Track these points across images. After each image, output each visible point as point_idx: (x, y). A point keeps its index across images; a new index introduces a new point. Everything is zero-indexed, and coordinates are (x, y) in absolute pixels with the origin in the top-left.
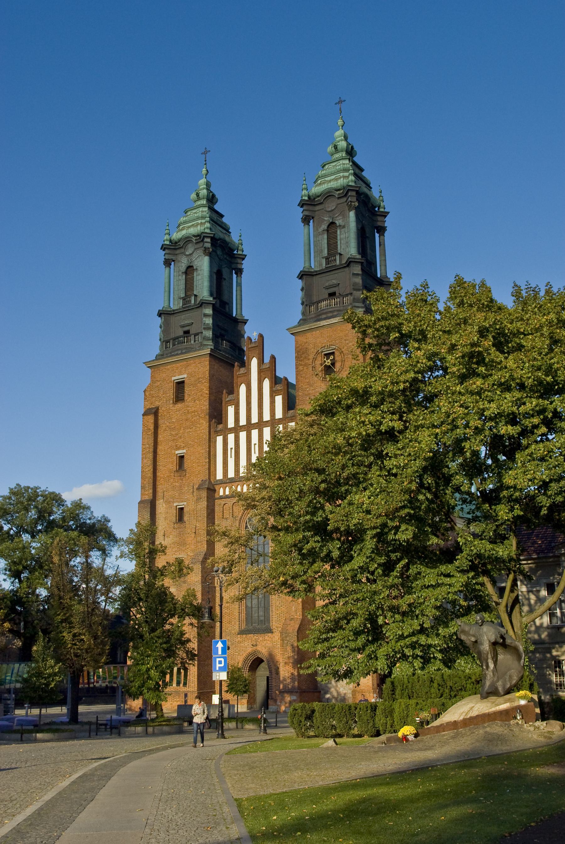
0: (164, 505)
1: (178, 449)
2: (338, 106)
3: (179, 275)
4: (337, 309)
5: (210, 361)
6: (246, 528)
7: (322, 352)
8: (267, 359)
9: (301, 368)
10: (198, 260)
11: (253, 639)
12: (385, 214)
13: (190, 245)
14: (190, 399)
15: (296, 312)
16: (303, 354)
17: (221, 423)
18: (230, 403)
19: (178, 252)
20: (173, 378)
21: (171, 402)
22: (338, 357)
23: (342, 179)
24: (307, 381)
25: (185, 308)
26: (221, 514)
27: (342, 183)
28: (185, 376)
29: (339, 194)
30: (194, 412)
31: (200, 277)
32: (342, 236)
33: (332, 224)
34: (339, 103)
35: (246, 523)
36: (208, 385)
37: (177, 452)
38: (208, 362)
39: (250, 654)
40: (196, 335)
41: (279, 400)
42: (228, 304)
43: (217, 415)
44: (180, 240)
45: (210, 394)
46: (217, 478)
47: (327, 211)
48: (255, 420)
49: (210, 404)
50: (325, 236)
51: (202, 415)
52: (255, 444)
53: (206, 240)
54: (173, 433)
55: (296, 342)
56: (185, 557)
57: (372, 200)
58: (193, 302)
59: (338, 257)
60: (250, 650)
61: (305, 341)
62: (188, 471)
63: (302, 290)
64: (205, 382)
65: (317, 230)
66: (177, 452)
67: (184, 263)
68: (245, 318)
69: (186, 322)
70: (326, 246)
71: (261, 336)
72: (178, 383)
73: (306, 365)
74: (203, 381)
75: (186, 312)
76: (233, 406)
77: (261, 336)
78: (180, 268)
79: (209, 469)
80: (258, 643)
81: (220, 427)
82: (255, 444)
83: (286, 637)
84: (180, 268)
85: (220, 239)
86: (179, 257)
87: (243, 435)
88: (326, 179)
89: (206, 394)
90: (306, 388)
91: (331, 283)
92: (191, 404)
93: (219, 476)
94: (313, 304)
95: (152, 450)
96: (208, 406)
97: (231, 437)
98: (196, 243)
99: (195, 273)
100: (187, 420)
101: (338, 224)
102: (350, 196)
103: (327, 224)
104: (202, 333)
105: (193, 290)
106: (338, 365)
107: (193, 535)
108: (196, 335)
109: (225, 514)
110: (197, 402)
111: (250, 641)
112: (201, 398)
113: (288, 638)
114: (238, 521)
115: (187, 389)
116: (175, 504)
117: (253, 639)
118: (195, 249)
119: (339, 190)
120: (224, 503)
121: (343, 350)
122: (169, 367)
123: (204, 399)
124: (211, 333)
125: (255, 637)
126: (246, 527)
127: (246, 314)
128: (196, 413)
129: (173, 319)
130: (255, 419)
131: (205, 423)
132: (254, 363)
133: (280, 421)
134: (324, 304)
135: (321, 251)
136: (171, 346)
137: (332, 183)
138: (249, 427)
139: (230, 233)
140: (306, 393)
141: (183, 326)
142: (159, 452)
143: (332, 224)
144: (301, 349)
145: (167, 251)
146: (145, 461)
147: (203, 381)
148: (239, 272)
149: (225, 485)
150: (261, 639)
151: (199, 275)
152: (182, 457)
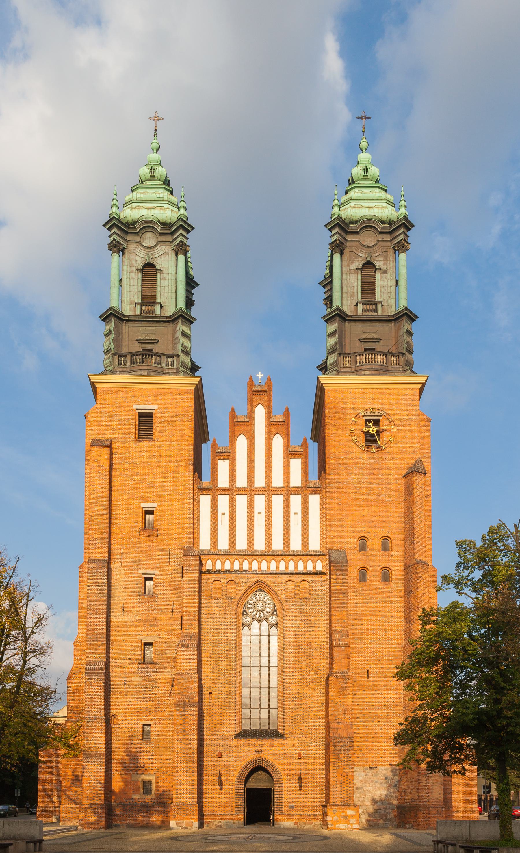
0: (122, 570)
1: (146, 501)
3: (131, 272)
7: (364, 416)
10: (163, 258)
13: (149, 235)
14: (164, 439)
19: (129, 238)
21: (133, 437)
22: (385, 425)
25: (146, 317)
32: (382, 283)
33: (368, 264)
36: (192, 426)
37: (143, 505)
39: (252, 762)
40: (168, 356)
41: (296, 464)
47: (363, 245)
48: (260, 482)
50: (360, 277)
54: (136, 479)
56: (157, 639)
58: (158, 313)
59: (379, 306)
60: (252, 757)
62: (161, 531)
66: (143, 505)
69: (147, 338)
72: (141, 416)
73: (340, 427)
74: (185, 420)
75: (147, 324)
76: (227, 461)
78: (134, 262)
84: (134, 262)
86: (132, 246)
89: (190, 437)
90: (340, 455)
93: (205, 544)
95: (107, 495)
96: (192, 453)
99: (158, 275)
100: (158, 465)
101: (377, 266)
103: (362, 263)
104: (178, 356)
106: (386, 437)
107: (169, 614)
108: (168, 356)
109: (214, 594)
114: (235, 604)
116: (140, 572)
118: (159, 242)
120: (214, 579)
123: (187, 443)
128: (174, 460)
129: (125, 327)
131: (187, 474)
133: (297, 491)
138: (251, 490)
140: (340, 461)
141: (140, 342)
142: (113, 501)
143: (368, 264)
147: (185, 420)
149: (216, 557)
150: (268, 744)
151: (164, 279)
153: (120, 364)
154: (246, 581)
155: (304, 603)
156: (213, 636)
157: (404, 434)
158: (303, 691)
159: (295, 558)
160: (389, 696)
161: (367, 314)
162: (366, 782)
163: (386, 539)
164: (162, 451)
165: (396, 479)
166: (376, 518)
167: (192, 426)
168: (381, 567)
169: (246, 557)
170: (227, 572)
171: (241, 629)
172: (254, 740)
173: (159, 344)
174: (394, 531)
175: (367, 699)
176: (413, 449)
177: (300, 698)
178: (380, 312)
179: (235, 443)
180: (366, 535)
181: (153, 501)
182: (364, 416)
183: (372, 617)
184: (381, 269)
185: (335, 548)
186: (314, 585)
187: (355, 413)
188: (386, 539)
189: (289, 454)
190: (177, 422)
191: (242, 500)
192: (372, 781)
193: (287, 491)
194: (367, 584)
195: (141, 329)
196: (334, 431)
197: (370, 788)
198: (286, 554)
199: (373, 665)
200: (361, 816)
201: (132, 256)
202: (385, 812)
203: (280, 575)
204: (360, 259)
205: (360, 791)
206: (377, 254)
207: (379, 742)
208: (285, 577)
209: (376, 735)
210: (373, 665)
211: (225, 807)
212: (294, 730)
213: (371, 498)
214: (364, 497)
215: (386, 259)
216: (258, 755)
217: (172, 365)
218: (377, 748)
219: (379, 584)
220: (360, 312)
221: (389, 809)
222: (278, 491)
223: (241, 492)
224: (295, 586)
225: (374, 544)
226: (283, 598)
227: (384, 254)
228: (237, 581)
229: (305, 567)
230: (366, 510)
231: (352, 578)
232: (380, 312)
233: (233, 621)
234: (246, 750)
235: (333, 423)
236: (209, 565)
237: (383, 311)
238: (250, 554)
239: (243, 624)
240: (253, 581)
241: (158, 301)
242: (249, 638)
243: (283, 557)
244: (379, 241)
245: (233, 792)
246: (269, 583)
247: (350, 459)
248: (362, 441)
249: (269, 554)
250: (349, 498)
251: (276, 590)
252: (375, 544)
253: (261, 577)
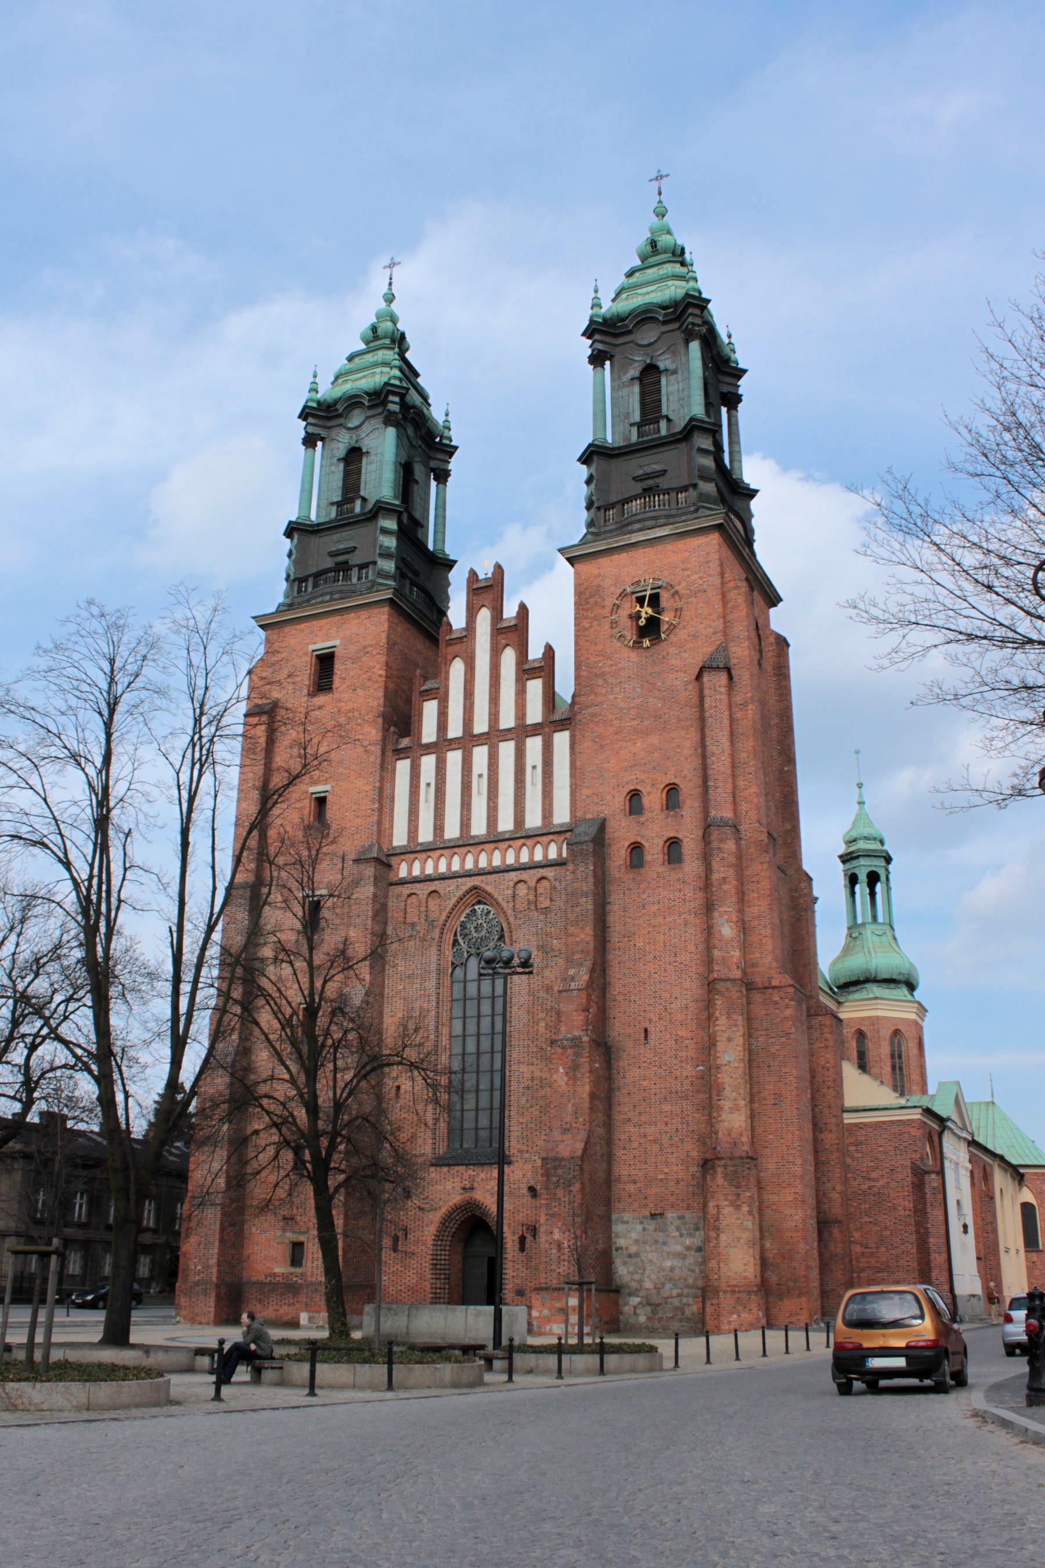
2: (655, 184)
3: (332, 465)
4: (664, 512)
5: (389, 615)
6: (454, 945)
7: (633, 593)
8: (510, 611)
9: (586, 624)
10: (372, 436)
11: (466, 1176)
12: (740, 373)
14: (345, 686)
15: (575, 526)
16: (591, 597)
17: (409, 735)
18: (428, 694)
21: (305, 692)
23: (673, 288)
24: (600, 648)
25: (339, 520)
26: (402, 914)
27: (673, 295)
28: (337, 642)
29: (665, 315)
30: (353, 710)
31: (373, 467)
34: (657, 179)
35: (455, 935)
38: (386, 617)
41: (535, 687)
42: (422, 526)
43: (399, 722)
44: (336, 402)
45: (387, 677)
46: (395, 843)
49: (385, 696)
50: (636, 389)
51: (370, 717)
52: (480, 776)
53: (391, 398)
55: (576, 573)
57: (719, 342)
59: (663, 424)
60: (457, 1198)
61: (596, 572)
63: (588, 482)
64: (379, 654)
65: (619, 378)
67: (342, 442)
68: (451, 558)
69: (342, 546)
70: (637, 406)
71: (499, 569)
73: (595, 618)
74: (374, 652)
77: (499, 569)
79: (379, 822)
80: (476, 1185)
81: (405, 742)
82: (480, 776)
83: (555, 1168)
84: (335, 452)
85: (414, 407)
86: (334, 433)
87: (454, 758)
88: (638, 291)
89: (381, 676)
90: (595, 662)
91: (648, 470)
92: (345, 696)
93: (400, 838)
94: (613, 506)
96: (382, 700)
97: (428, 763)
98: (370, 408)
99: (364, 460)
101: (662, 368)
102: (691, 314)
103: (640, 369)
104: (375, 563)
105: (359, 490)
109: (408, 916)
110: (359, 691)
111: (457, 1179)
112: (369, 684)
113: (560, 1172)
114: (437, 931)
115: (339, 667)
117: (466, 1176)
118: (368, 418)
119: (664, 308)
120: (408, 892)
121: (677, 588)
122: (302, 626)
123: (376, 686)
124: (393, 565)
125: (470, 1172)
126: (455, 942)
127: (451, 551)
128: (356, 714)
129: (315, 541)
130: (481, 726)
132: (484, 616)
133: (535, 730)
134: (636, 505)
135: (628, 415)
136: (310, 589)
137: (651, 296)
138: (468, 741)
139: (429, 405)
140: (596, 670)
141: (333, 555)
144: (586, 589)
145: (311, 420)
146: (244, 805)
147: (374, 652)
148: (442, 477)
149: (413, 856)
150: (483, 1175)
151: (371, 463)
152: (321, 802)
153: (299, 591)
154: (454, 890)
155: (542, 917)
156: (404, 988)
157: (696, 609)
158: (539, 1074)
159: (530, 842)
160: (685, 1074)
161: (645, 439)
162: (645, 1243)
163: (672, 790)
164: (342, 704)
165: (686, 683)
166: (656, 754)
167: (383, 659)
168: (665, 838)
169: (455, 850)
170: (429, 879)
171: (450, 971)
172: (462, 1168)
173: (357, 552)
174: (686, 772)
175: (645, 1083)
176: (711, 630)
177: (535, 1087)
178: (664, 432)
179: (447, 673)
180: (638, 788)
181: (326, 781)
182: (633, 593)
183: (651, 929)
184: (666, 370)
185: (589, 816)
186: (557, 884)
187: (619, 591)
188: (672, 790)
189: (525, 672)
190: (364, 659)
191: (454, 758)
192: (656, 1242)
193: (522, 732)
194: (642, 871)
195: (336, 537)
196: (587, 625)
197: (653, 1256)
198: (522, 835)
199: (655, 1018)
200: (638, 1311)
201: (334, 445)
202: (681, 1302)
203: (506, 874)
204: (636, 365)
205: (634, 1260)
206: (660, 352)
207: (667, 1163)
208: (514, 876)
209: (661, 1150)
210: (655, 1018)
211: (412, 1289)
212: (525, 1148)
213: (646, 723)
214: (635, 723)
215: (675, 354)
216: (468, 1195)
217: (367, 577)
218: (662, 1176)
219: (661, 869)
220: (634, 438)
221: (687, 1296)
222: (506, 735)
223: (454, 746)
224: (529, 888)
225: (653, 799)
226: (510, 912)
227: (671, 350)
228: (441, 892)
229: (545, 855)
230: (639, 745)
231: (617, 863)
232: (664, 432)
233: (434, 959)
234: (449, 1187)
235: (585, 613)
236: (403, 872)
237: (668, 429)
238: (466, 843)
239: (453, 964)
240: (465, 888)
241: (362, 493)
242: (462, 985)
243: (511, 843)
244: (664, 333)
245: (427, 1265)
246: (489, 889)
247: (612, 665)
248: (631, 635)
249: (494, 840)
250: (611, 730)
251: (500, 900)
252: (653, 799)
253: (476, 881)
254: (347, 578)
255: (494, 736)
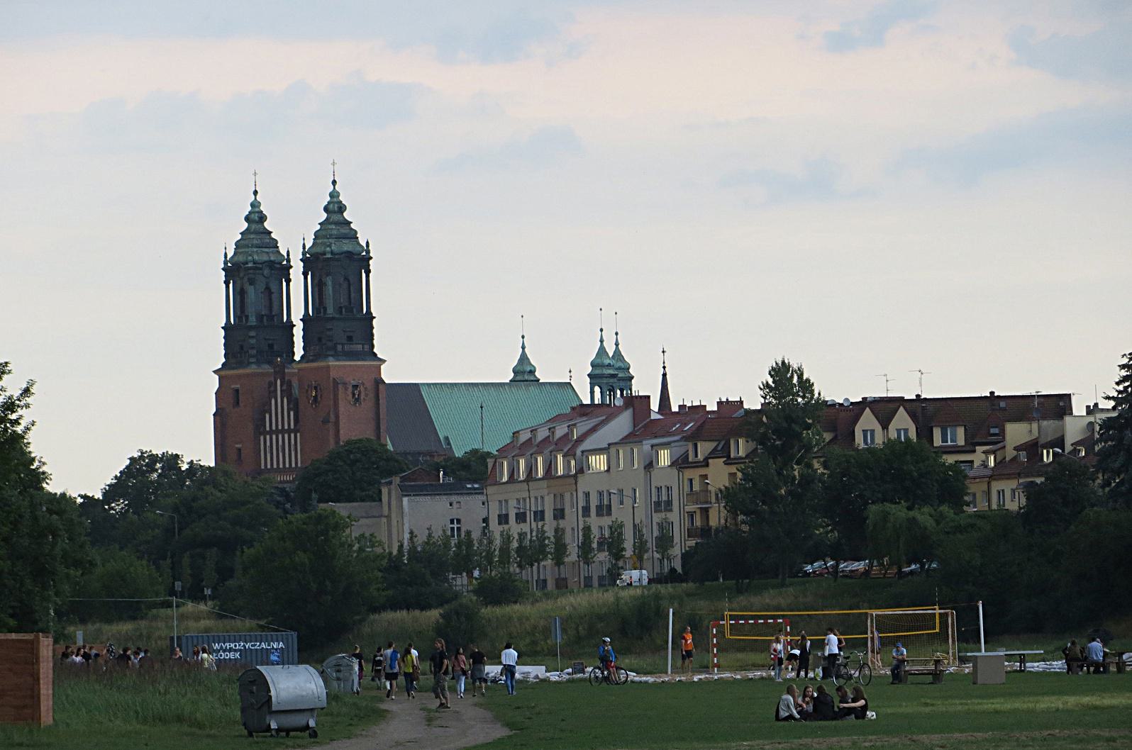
18: (266, 412)
20: (233, 386)
28: (238, 386)
93: (263, 467)
138: (277, 432)
152: (239, 450)
193: (289, 431)
254: (241, 357)
255: (283, 431)
